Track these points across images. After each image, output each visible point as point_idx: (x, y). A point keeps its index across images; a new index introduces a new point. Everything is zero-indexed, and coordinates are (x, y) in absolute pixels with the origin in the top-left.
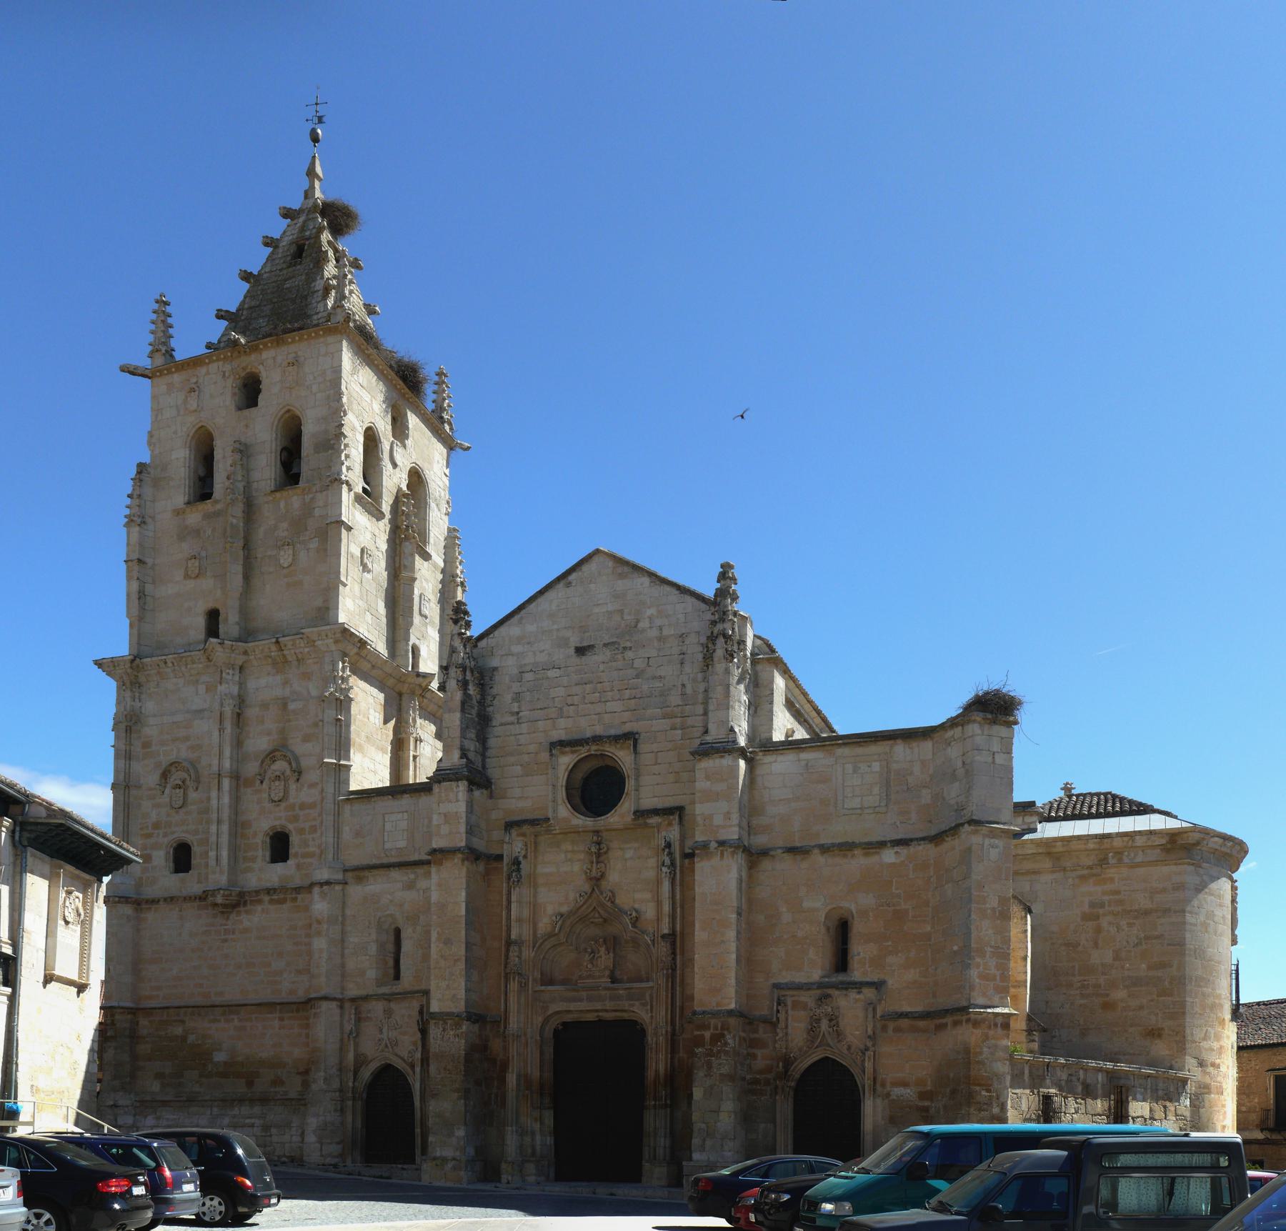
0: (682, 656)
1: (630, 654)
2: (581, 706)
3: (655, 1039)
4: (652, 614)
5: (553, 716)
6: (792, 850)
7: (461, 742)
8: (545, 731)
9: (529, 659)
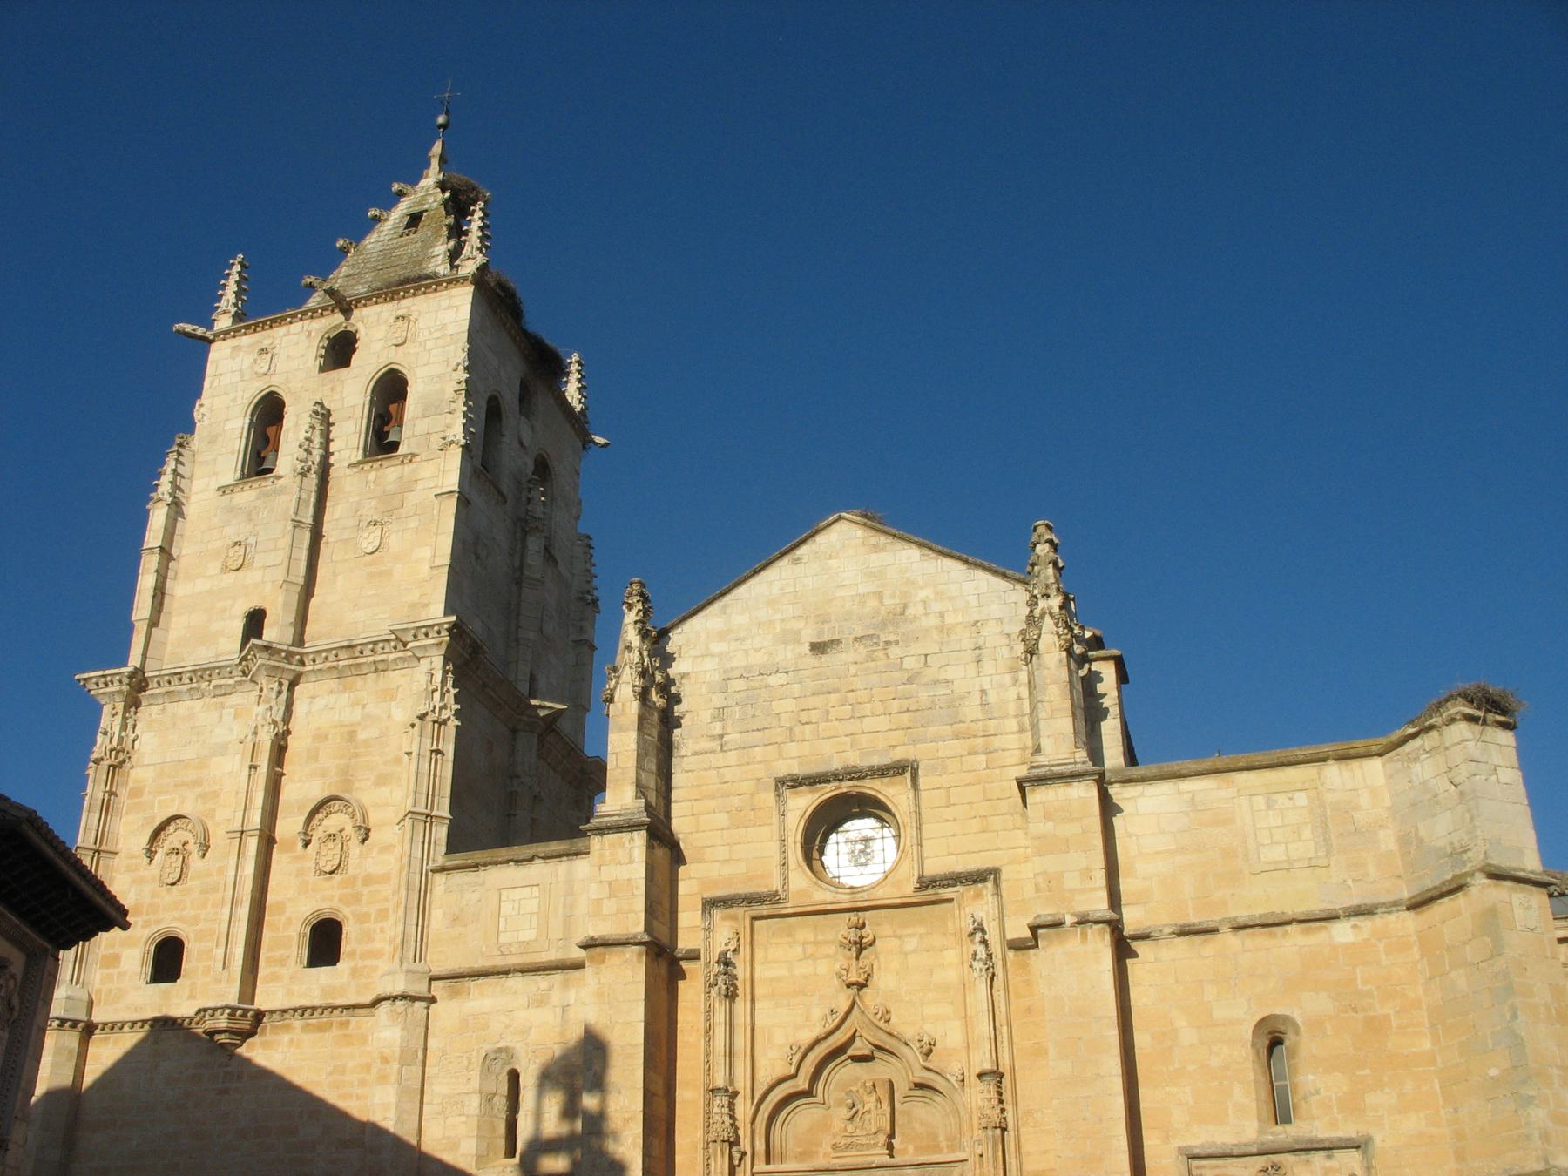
0: (978, 651)
1: (895, 652)
2: (822, 725)
4: (927, 597)
5: (779, 739)
8: (765, 762)
9: (738, 661)
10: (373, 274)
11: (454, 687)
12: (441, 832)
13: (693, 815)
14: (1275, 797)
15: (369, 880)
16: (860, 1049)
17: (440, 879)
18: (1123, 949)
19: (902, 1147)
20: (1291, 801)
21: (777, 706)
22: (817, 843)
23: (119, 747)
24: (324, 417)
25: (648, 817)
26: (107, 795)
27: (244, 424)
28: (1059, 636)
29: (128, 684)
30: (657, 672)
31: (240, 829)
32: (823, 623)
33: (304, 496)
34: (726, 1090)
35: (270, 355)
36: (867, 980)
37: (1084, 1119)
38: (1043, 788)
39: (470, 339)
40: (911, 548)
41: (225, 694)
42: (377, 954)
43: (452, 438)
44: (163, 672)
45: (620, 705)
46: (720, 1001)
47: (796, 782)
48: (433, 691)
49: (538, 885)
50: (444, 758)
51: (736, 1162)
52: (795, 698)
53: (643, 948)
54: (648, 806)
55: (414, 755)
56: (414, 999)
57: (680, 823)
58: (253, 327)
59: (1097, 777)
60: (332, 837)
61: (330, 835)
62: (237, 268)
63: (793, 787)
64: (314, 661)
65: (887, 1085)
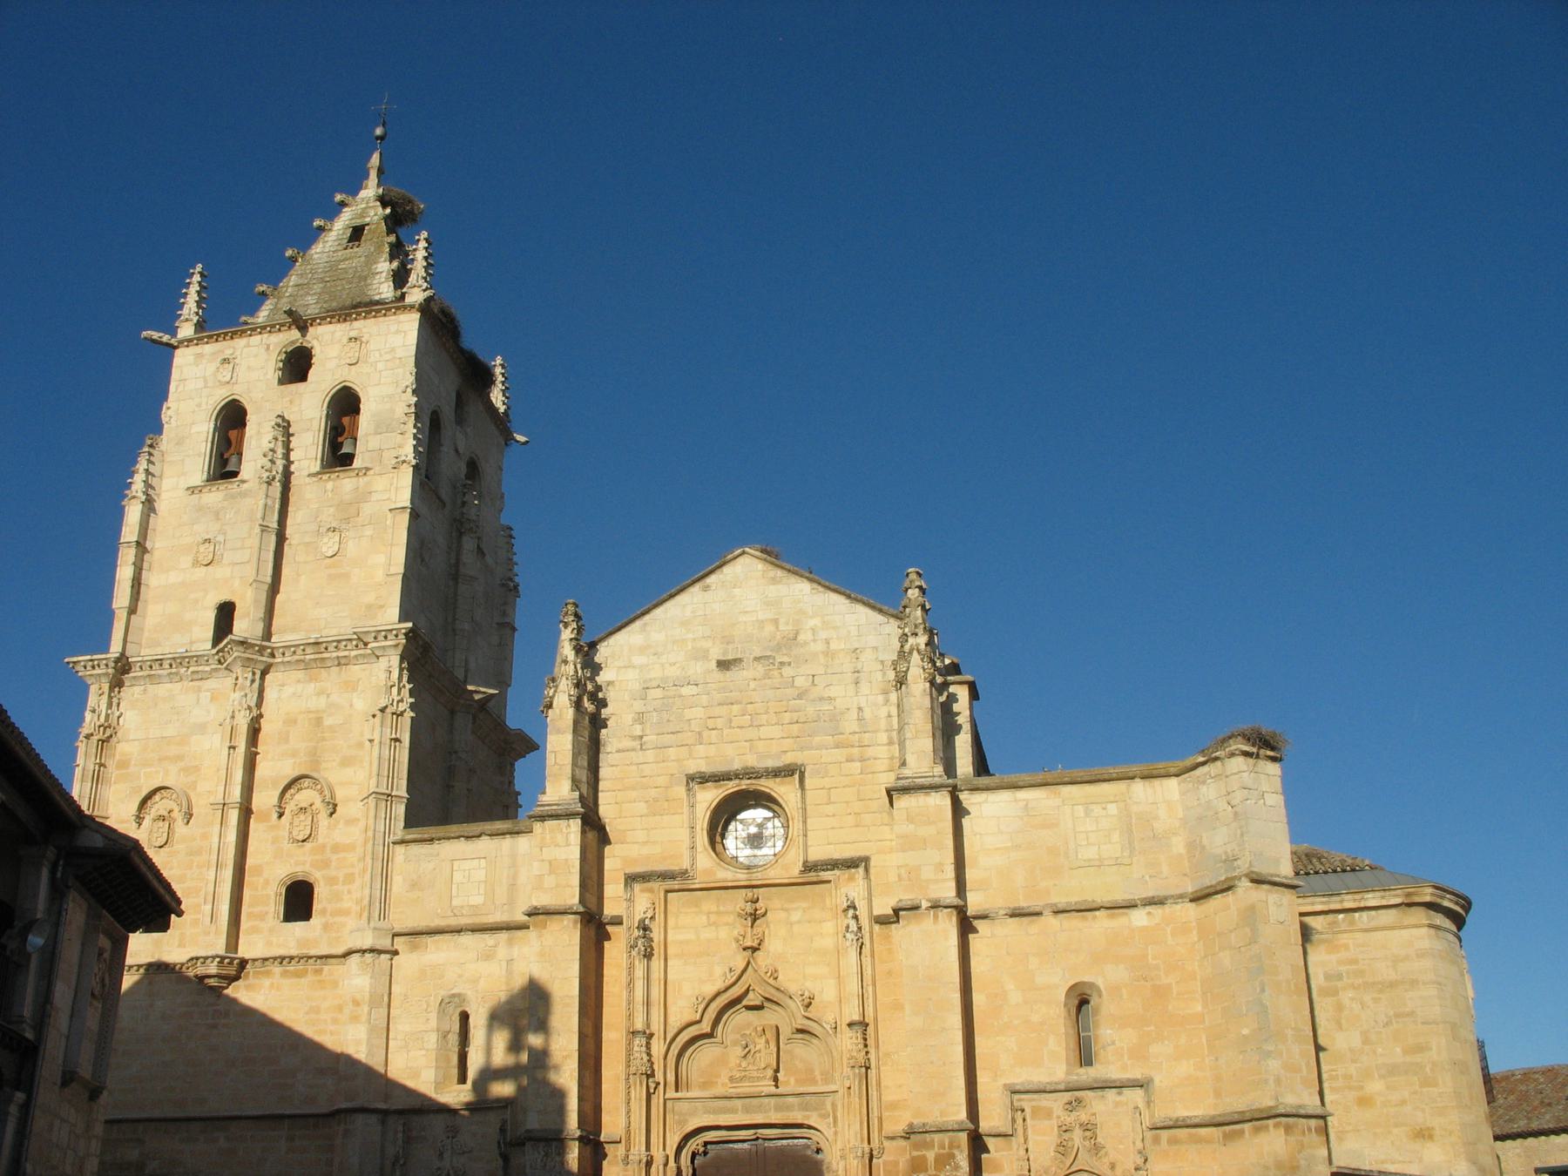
0: (856, 674)
1: (787, 671)
3: (842, 1164)
4: (815, 625)
6: (1016, 914)
7: (573, 770)
8: (677, 760)
9: (656, 673)
10: (321, 285)
11: (408, 682)
12: (400, 810)
13: (617, 803)
14: (1093, 806)
15: (336, 848)
16: (752, 1000)
17: (400, 849)
18: (966, 926)
19: (786, 1079)
20: (1104, 811)
21: (688, 714)
22: (719, 830)
23: (106, 724)
24: (285, 428)
25: (582, 807)
26: (97, 766)
27: (209, 428)
28: (924, 670)
29: (114, 668)
30: (588, 682)
31: (223, 802)
32: (728, 644)
33: (270, 502)
34: (645, 1033)
35: (232, 365)
36: (759, 944)
37: (932, 1063)
38: (907, 796)
39: (417, 364)
40: (803, 582)
41: (201, 679)
42: (346, 913)
43: (403, 458)
44: (145, 658)
45: (558, 711)
46: (640, 960)
47: (703, 779)
48: (391, 687)
49: (485, 858)
50: (402, 745)
51: (652, 1091)
52: (704, 707)
53: (578, 917)
54: (581, 797)
55: (377, 742)
56: (380, 952)
57: (606, 810)
58: (215, 337)
59: (950, 789)
60: (303, 810)
61: (301, 809)
62: (197, 278)
63: (701, 783)
64: (284, 654)
65: (774, 1030)
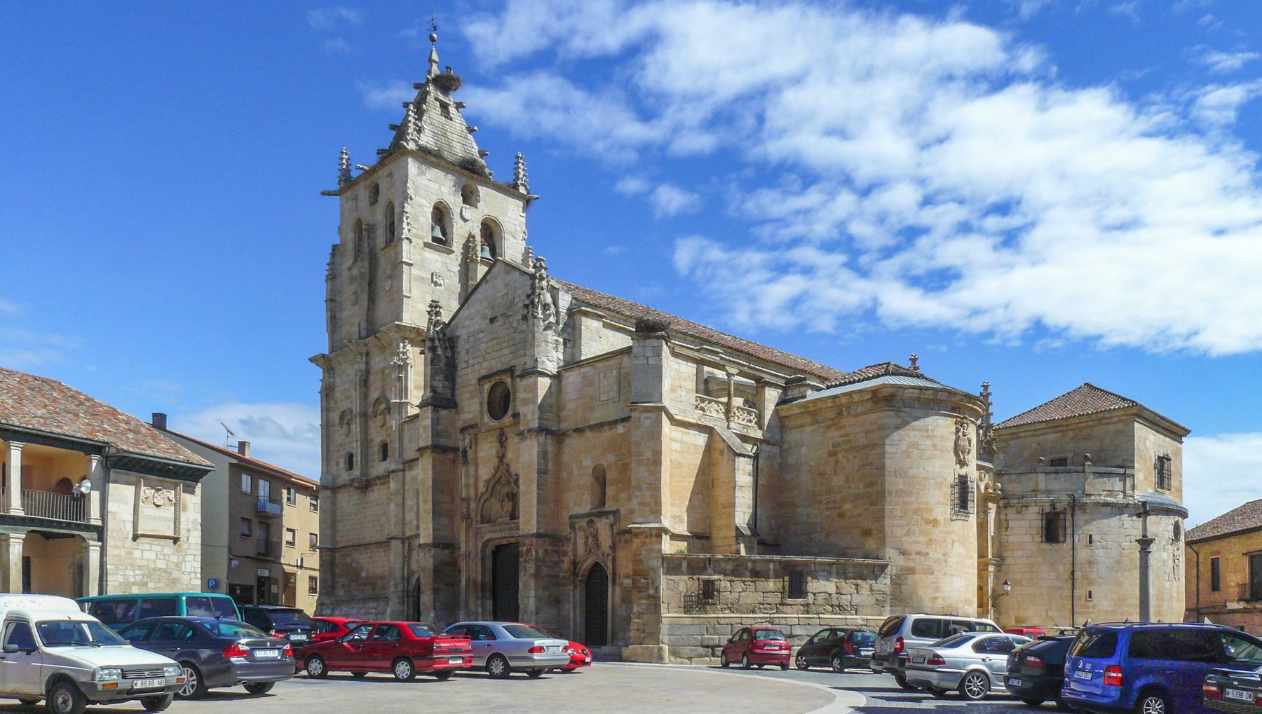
1: (511, 319)
5: (482, 361)
6: (577, 430)
